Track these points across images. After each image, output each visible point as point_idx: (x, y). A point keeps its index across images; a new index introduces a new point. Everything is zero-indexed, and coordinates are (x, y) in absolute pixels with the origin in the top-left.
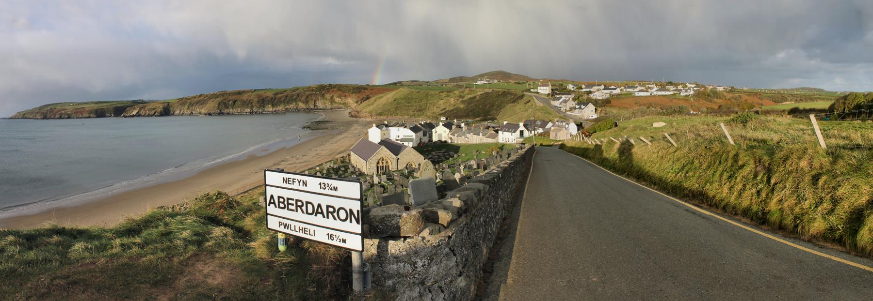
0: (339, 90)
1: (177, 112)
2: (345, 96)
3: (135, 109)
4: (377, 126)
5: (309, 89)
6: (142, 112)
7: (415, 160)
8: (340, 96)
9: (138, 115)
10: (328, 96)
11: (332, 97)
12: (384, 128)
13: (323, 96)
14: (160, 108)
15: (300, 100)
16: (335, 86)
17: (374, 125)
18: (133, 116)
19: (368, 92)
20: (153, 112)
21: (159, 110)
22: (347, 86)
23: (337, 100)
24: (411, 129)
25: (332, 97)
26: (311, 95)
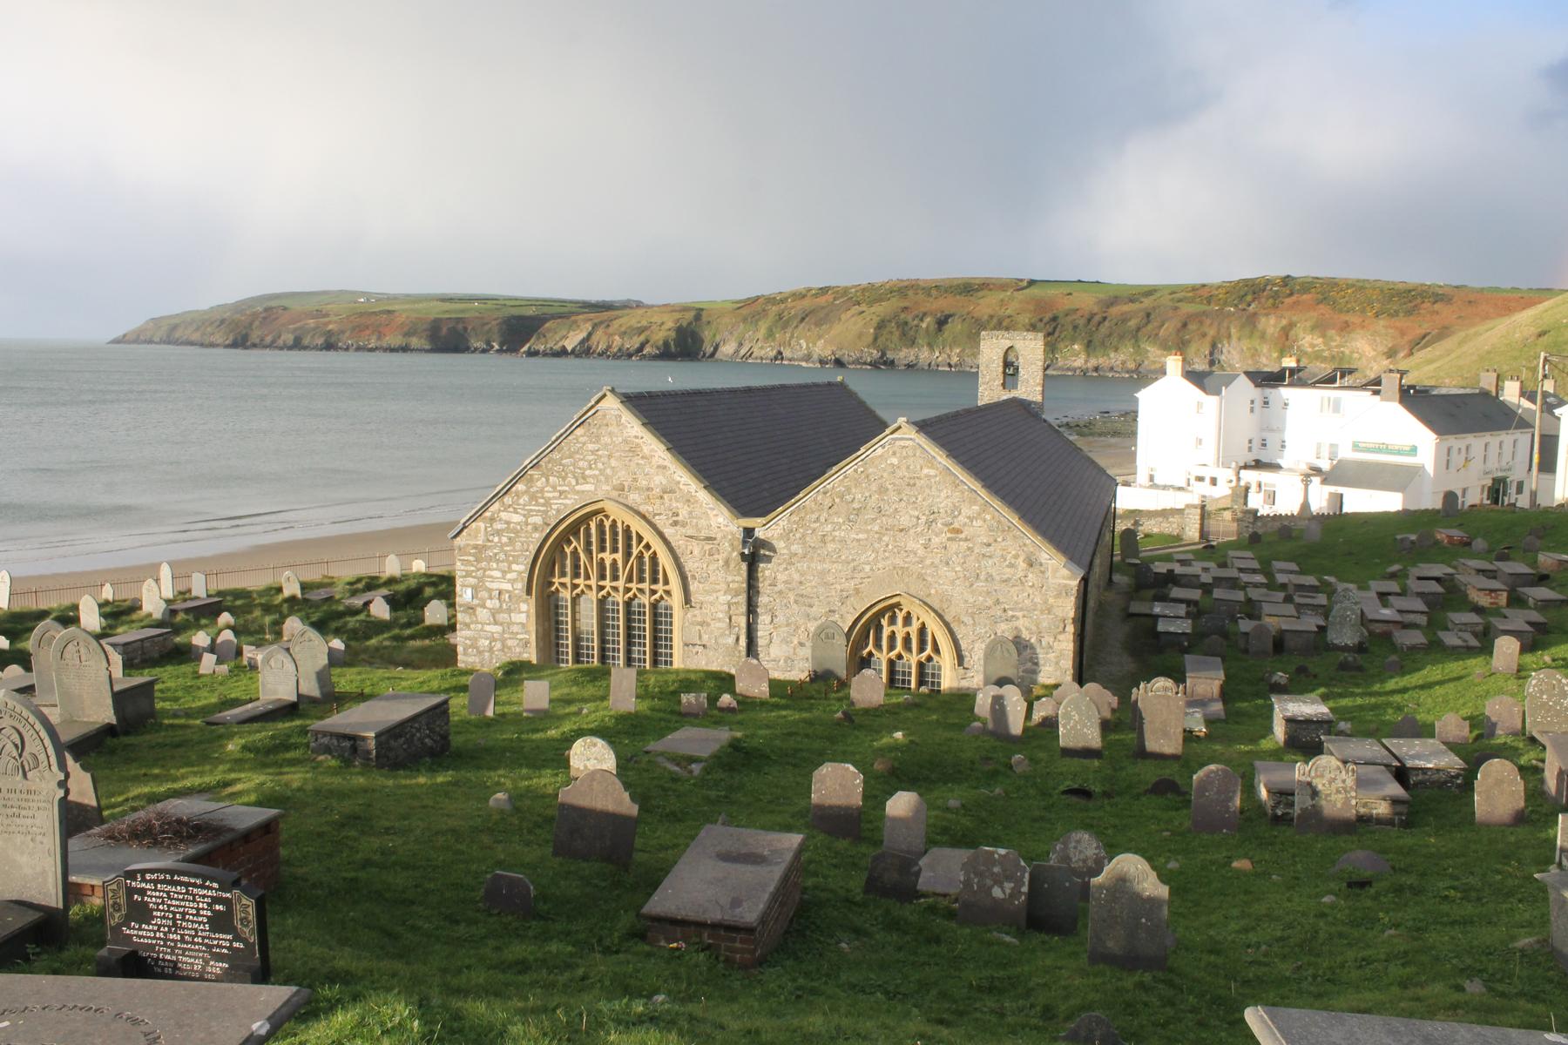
0: (1324, 300)
1: (727, 349)
2: (1345, 328)
3: (574, 326)
4: (1196, 378)
5: (1200, 293)
6: (600, 342)
7: (960, 599)
8: (1320, 327)
9: (584, 351)
10: (1271, 324)
11: (1286, 332)
12: (1244, 388)
13: (1252, 320)
14: (664, 330)
15: (1153, 338)
16: (1308, 285)
17: (1173, 364)
18: (563, 353)
19: (1446, 312)
20: (635, 342)
21: (659, 336)
22: (1359, 287)
23: (1308, 340)
24: (1416, 399)
25: (1286, 332)
26: (1199, 317)
